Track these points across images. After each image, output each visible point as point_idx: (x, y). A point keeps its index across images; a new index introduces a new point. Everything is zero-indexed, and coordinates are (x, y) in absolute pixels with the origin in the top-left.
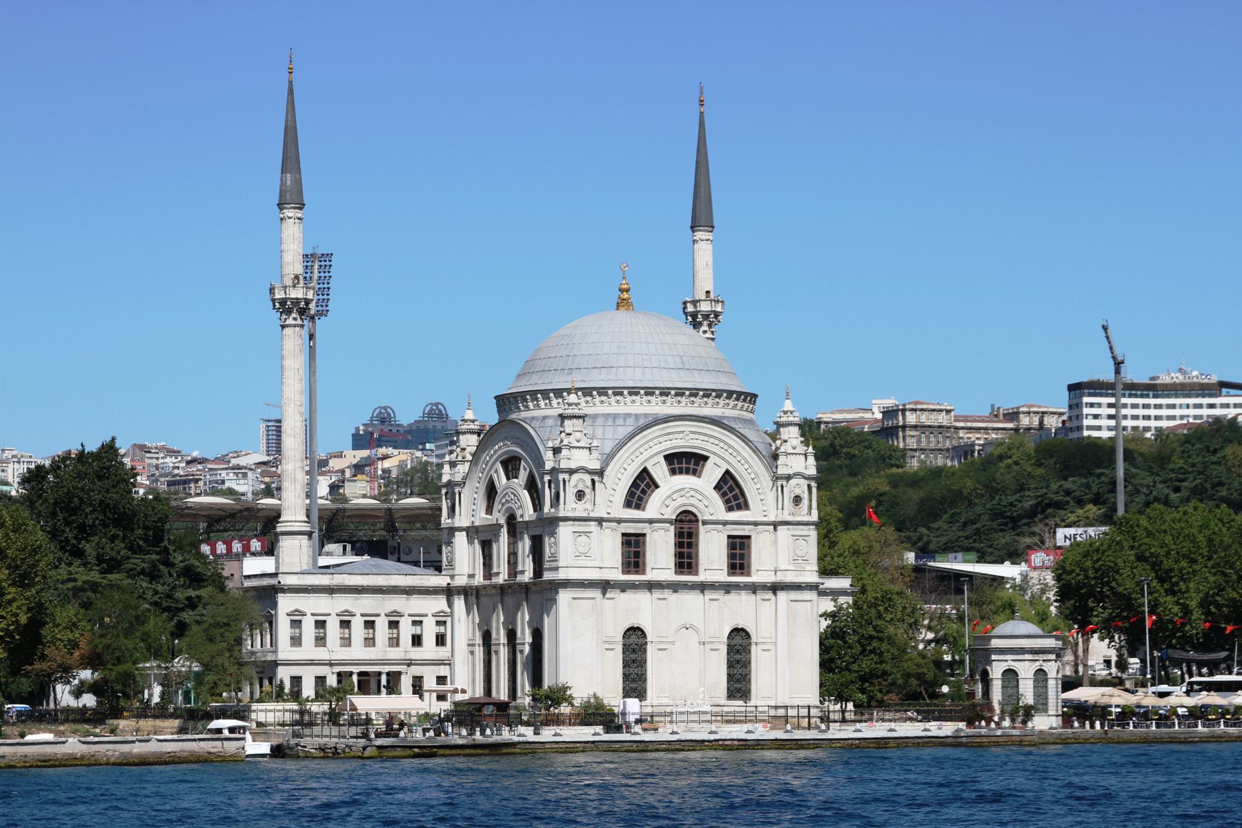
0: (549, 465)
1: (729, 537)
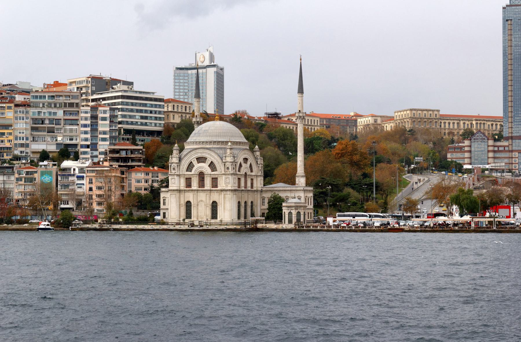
1: (212, 178)
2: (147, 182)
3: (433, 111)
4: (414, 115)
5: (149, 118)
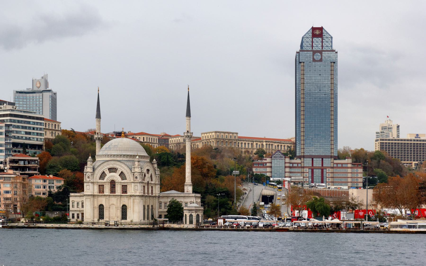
2: (44, 188)
3: (233, 133)
4: (218, 137)
5: (32, 133)
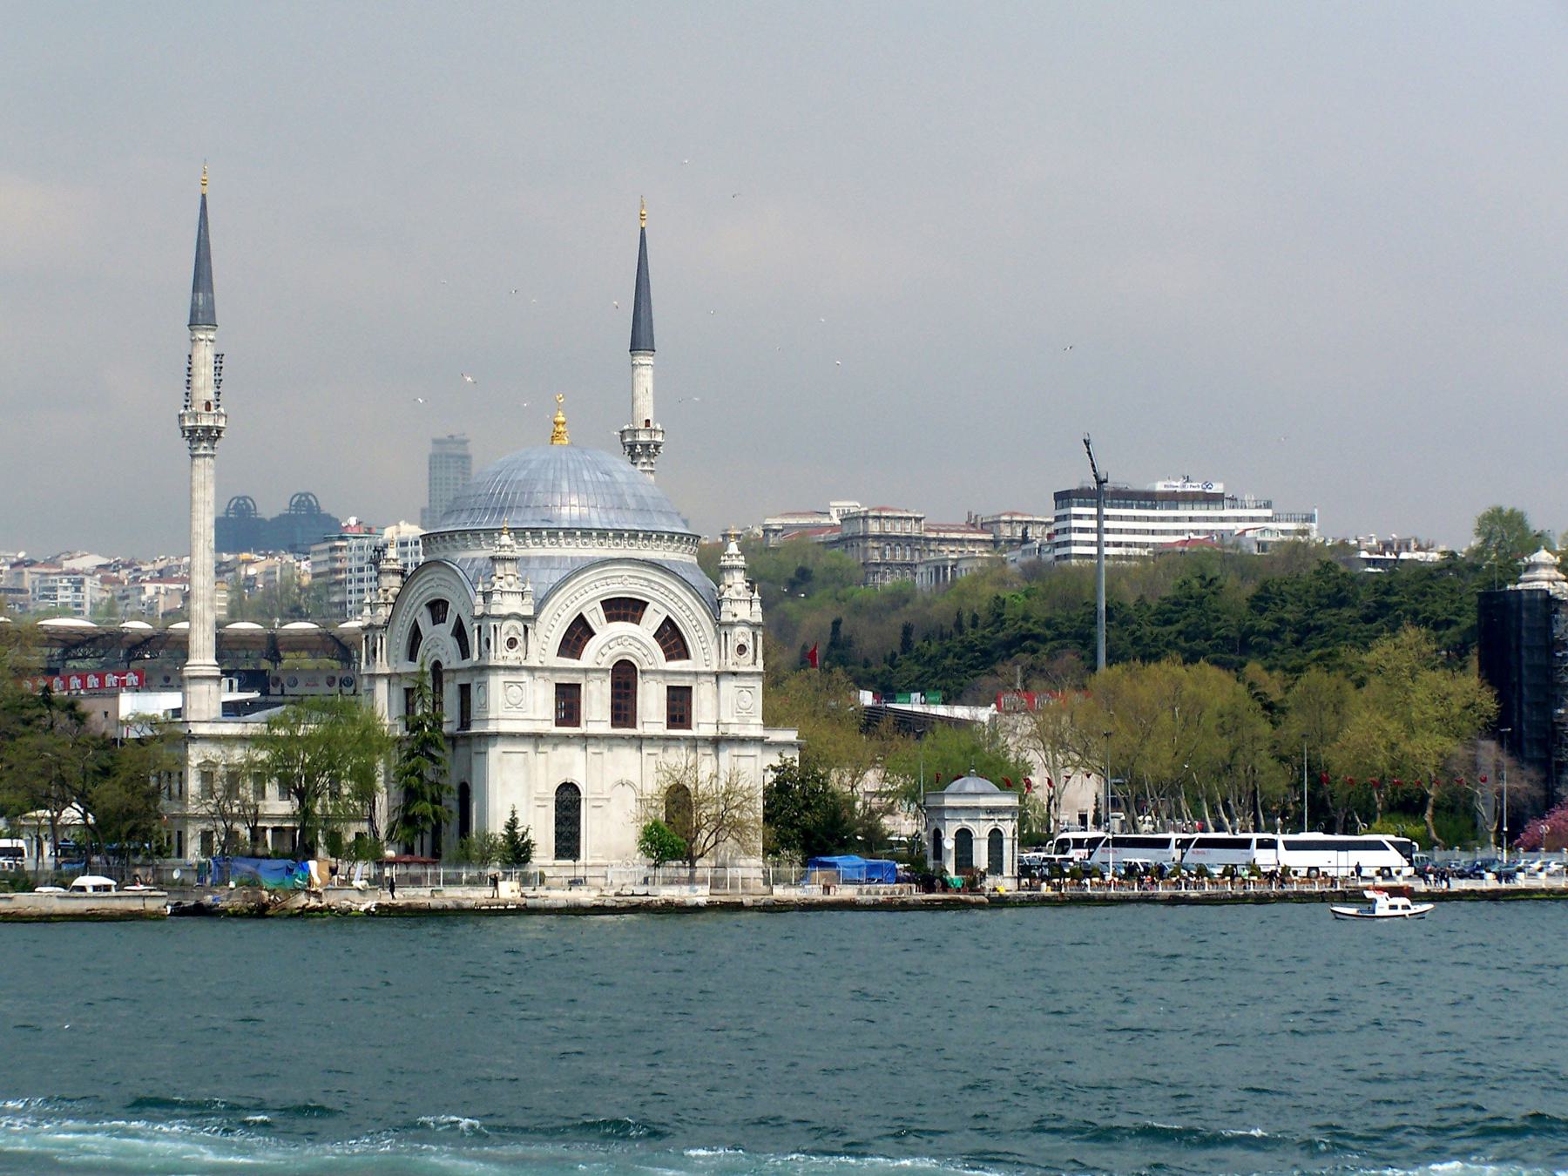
0: (478, 611)
